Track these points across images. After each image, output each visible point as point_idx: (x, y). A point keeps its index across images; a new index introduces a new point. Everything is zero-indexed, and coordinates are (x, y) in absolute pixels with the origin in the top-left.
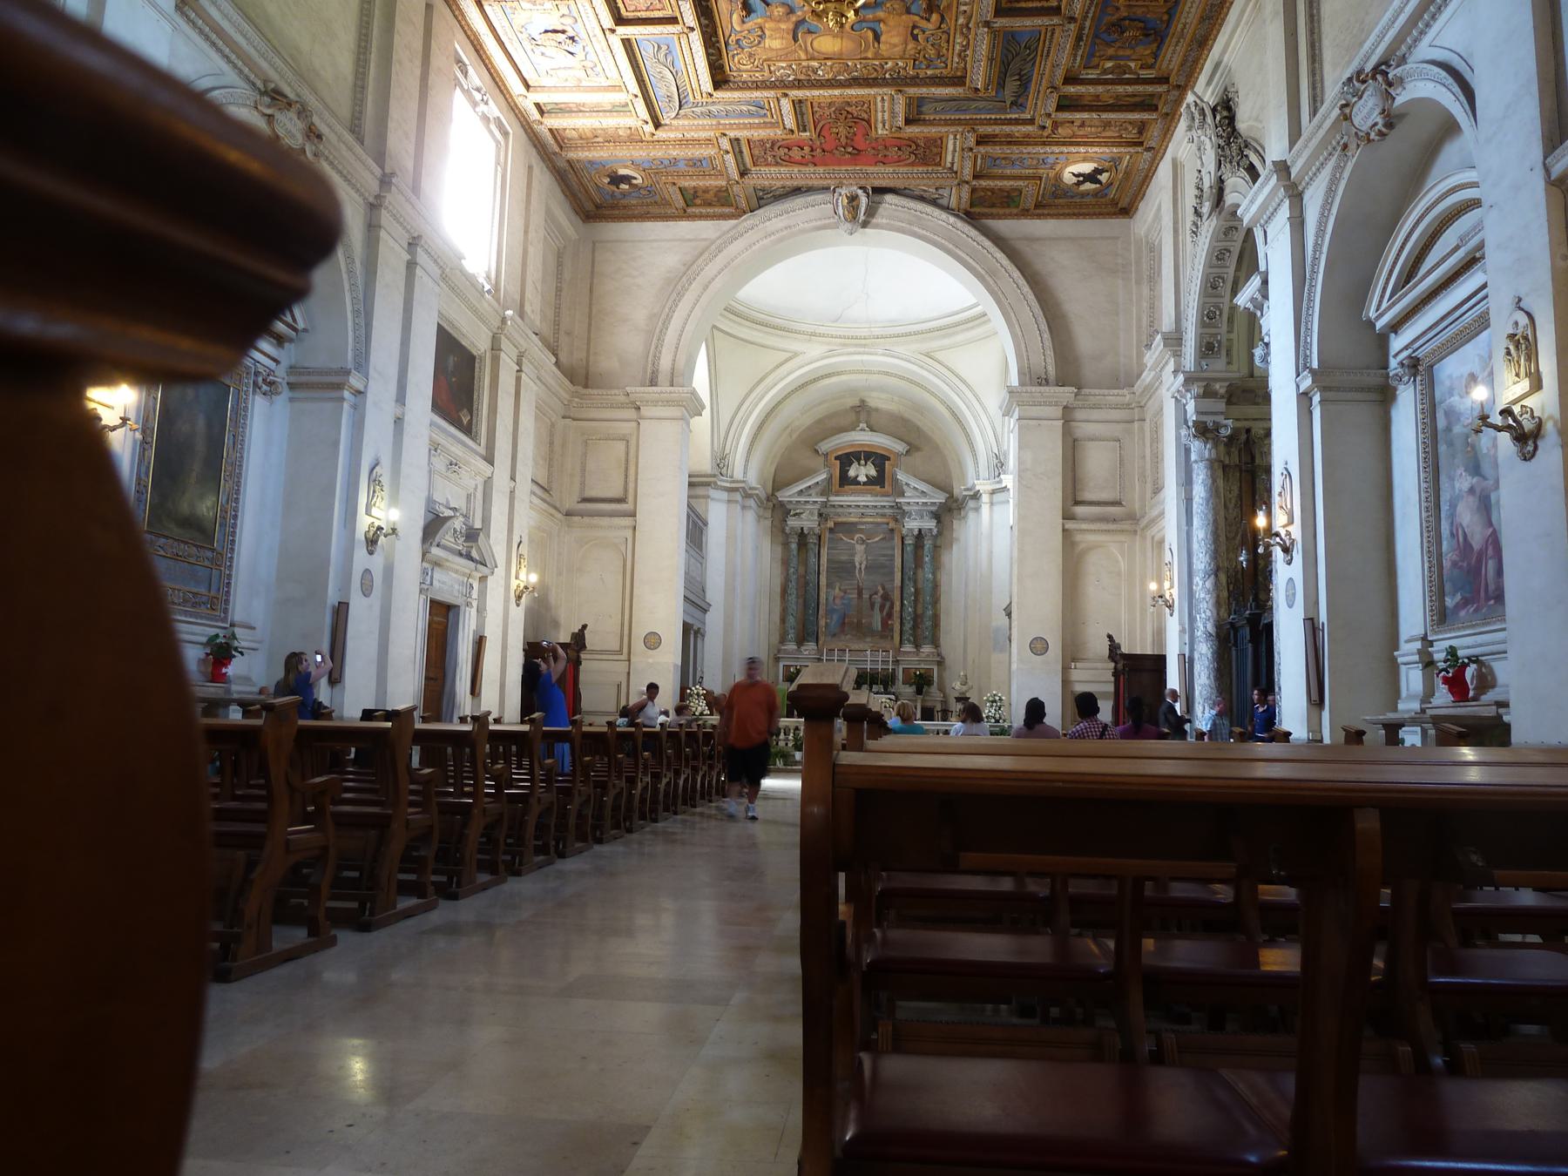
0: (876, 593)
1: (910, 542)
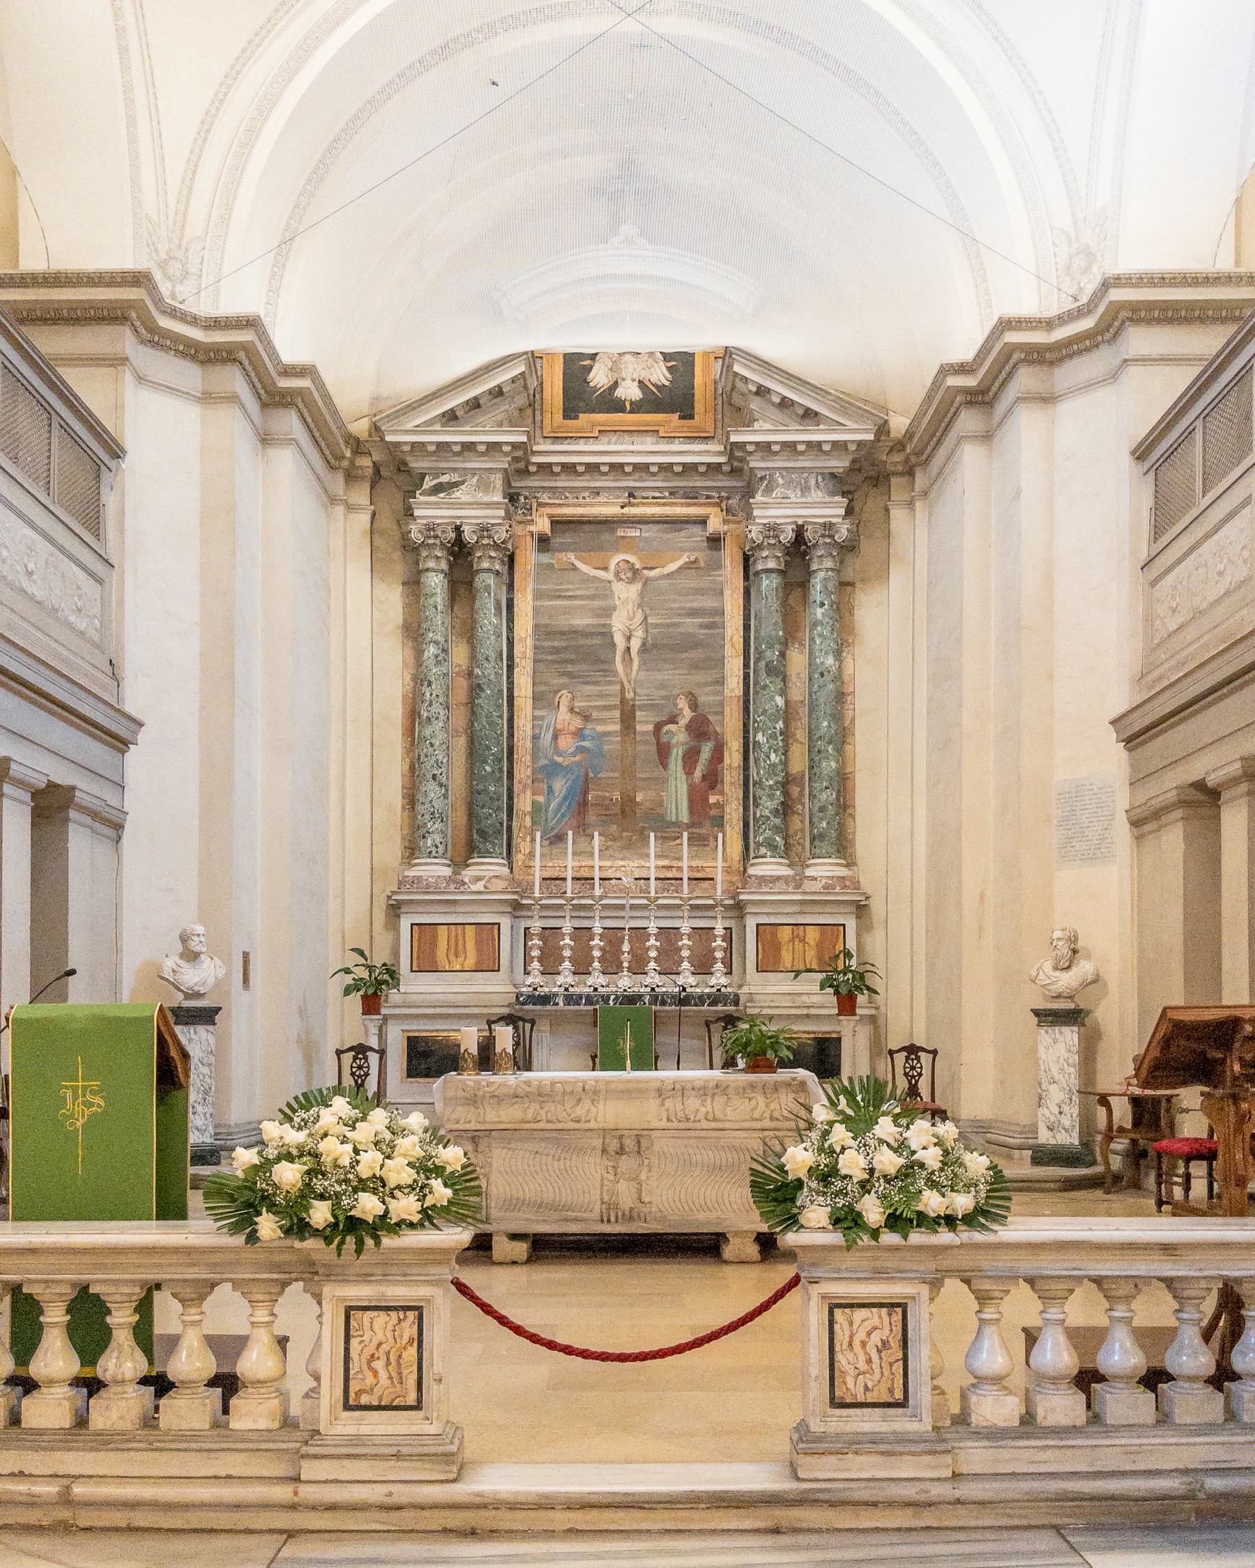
0: (673, 720)
1: (771, 564)
